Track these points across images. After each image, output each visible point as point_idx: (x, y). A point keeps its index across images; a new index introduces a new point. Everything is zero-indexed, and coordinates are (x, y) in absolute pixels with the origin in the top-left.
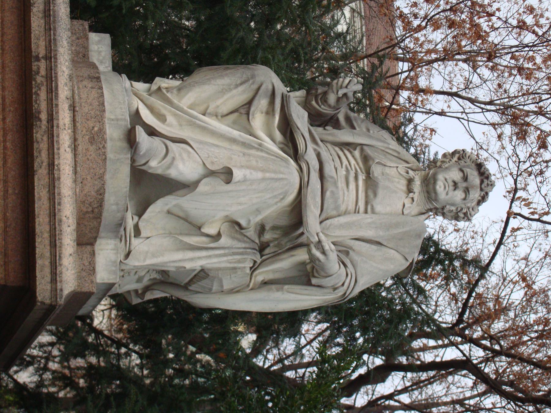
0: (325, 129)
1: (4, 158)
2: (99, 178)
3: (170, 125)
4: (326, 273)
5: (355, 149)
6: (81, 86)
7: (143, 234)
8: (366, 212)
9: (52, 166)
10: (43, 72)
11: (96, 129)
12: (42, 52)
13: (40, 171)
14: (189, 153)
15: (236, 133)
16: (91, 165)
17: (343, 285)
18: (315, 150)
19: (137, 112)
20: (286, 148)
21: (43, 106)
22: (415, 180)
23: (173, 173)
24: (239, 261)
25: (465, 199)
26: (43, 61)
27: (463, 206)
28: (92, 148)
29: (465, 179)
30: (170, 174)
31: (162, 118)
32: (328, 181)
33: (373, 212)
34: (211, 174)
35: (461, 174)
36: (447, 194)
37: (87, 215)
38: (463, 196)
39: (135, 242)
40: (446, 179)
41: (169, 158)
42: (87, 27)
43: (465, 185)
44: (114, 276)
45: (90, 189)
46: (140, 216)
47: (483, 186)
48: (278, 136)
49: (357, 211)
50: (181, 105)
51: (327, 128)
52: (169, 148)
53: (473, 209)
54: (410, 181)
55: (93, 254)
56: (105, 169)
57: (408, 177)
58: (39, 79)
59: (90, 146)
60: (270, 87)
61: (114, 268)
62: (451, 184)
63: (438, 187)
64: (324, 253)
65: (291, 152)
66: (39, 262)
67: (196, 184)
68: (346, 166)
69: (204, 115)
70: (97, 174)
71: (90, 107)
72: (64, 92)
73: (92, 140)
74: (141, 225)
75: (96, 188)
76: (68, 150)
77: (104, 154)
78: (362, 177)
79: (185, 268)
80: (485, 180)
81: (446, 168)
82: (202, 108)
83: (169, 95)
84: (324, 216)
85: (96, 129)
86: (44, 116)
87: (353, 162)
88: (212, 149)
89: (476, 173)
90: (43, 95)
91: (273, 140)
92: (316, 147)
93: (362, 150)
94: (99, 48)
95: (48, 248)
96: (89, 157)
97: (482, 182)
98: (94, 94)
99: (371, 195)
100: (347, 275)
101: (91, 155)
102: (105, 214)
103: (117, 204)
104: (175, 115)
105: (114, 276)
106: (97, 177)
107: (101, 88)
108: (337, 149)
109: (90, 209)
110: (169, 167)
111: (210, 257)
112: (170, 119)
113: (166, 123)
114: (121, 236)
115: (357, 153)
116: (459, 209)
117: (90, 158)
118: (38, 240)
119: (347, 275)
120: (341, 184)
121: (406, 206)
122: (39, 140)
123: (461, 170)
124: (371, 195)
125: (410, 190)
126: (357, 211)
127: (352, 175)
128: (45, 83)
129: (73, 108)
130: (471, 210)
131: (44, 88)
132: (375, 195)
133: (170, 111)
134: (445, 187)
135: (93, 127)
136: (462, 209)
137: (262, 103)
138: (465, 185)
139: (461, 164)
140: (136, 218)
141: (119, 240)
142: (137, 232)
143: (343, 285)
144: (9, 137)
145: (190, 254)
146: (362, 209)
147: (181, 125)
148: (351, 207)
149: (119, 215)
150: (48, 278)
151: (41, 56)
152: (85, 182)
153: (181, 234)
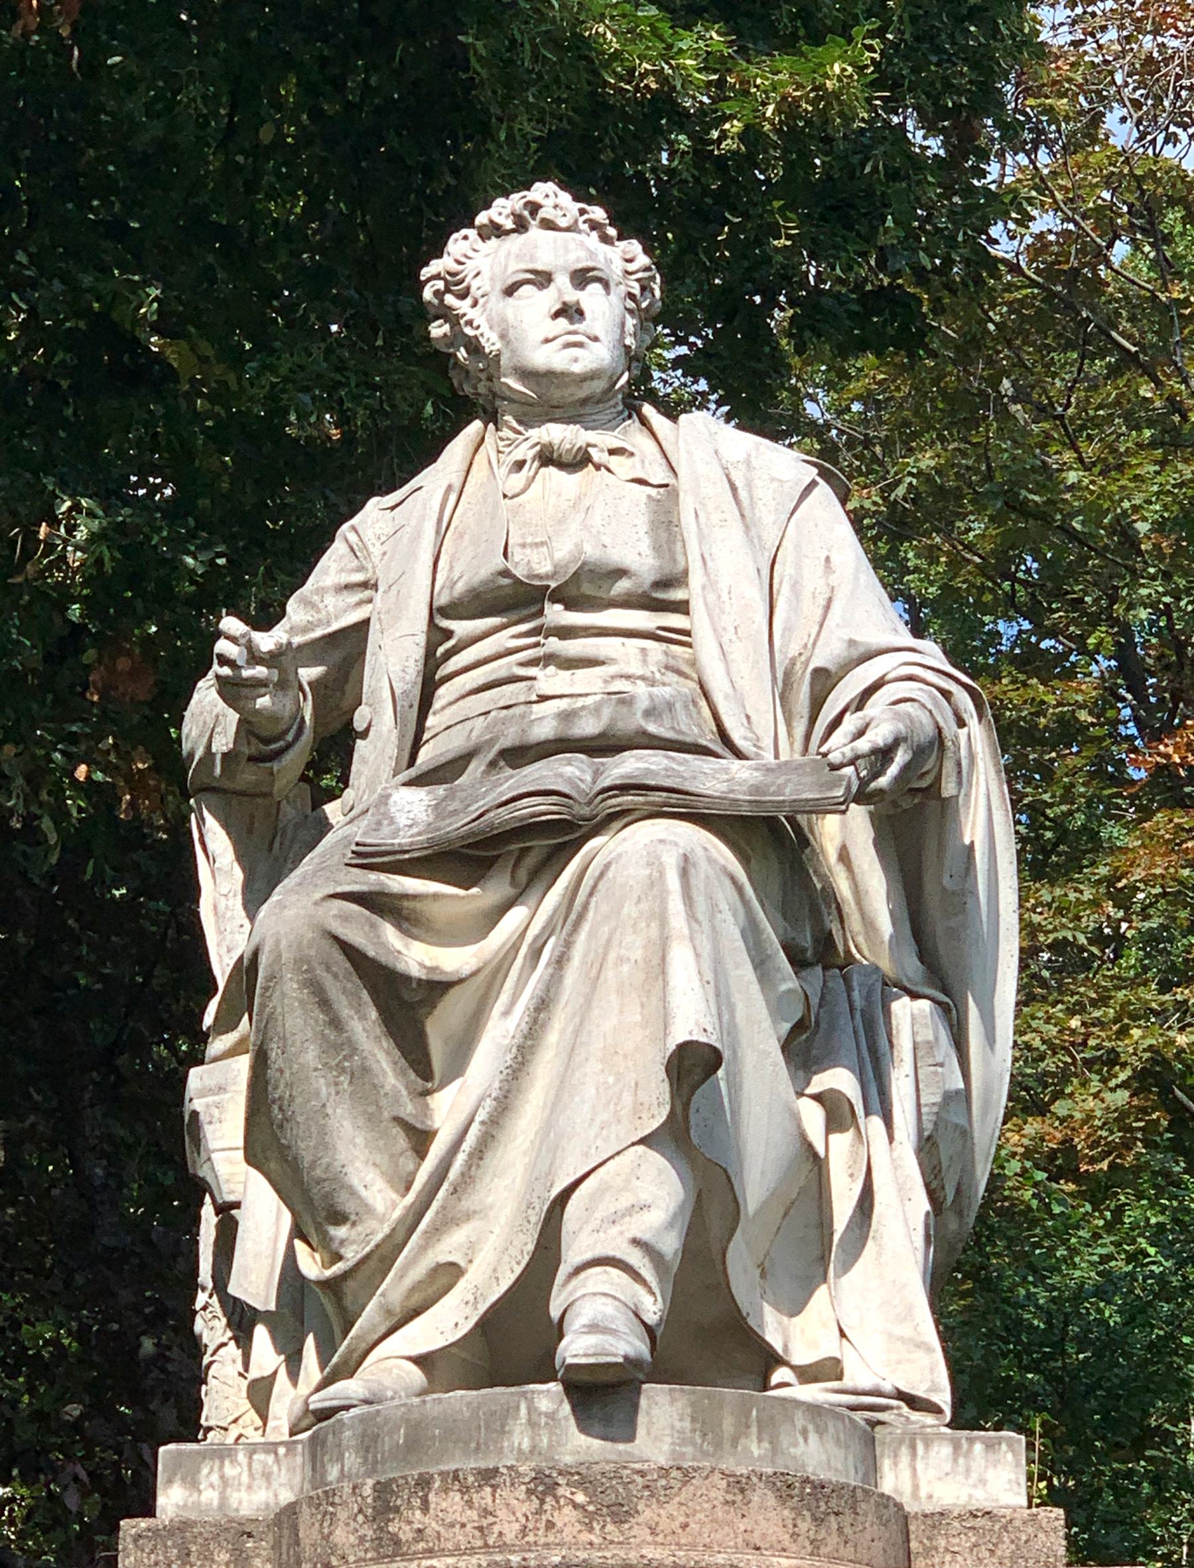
0: (364, 735)
2: (742, 1491)
3: (472, 1247)
4: (931, 743)
5: (449, 634)
8: (682, 607)
11: (580, 1498)
14: (604, 1189)
16: (700, 1516)
17: (946, 694)
19: (420, 1361)
20: (530, 861)
22: (545, 439)
23: (670, 1245)
25: (606, 285)
27: (623, 289)
28: (647, 1514)
29: (543, 279)
30: (676, 1253)
32: (610, 726)
35: (526, 290)
36: (596, 339)
37: (848, 1530)
38: (596, 287)
39: (857, 1375)
40: (547, 341)
41: (636, 1258)
42: (143, 1523)
43: (562, 281)
44: (1004, 1447)
47: (563, 223)
50: (397, 1214)
51: (359, 724)
52: (588, 1256)
53: (630, 261)
54: (548, 457)
57: (536, 464)
59: (640, 1519)
61: (978, 1447)
62: (562, 322)
63: (577, 368)
65: (542, 844)
68: (522, 664)
70: (730, 1497)
73: (620, 1513)
74: (802, 1356)
75: (771, 1501)
78: (556, 614)
79: (928, 1213)
80: (542, 214)
81: (503, 337)
82: (402, 1141)
83: (352, 1255)
84: (718, 748)
85: (580, 1498)
87: (504, 639)
89: (515, 242)
92: (476, 767)
93: (454, 610)
94: (212, 1486)
96: (677, 1523)
97: (548, 225)
99: (622, 586)
100: (911, 678)
101: (671, 1517)
104: (436, 1231)
105: (1004, 1447)
106: (739, 1497)
108: (444, 694)
112: (448, 1249)
113: (462, 1264)
114: (868, 1422)
115: (462, 628)
116: (631, 304)
117: (682, 1519)
119: (911, 678)
120: (586, 680)
121: (641, 475)
123: (510, 291)
124: (622, 586)
127: (553, 644)
130: (631, 267)
133: (423, 1249)
134: (579, 345)
135: (576, 1506)
136: (631, 296)
139: (486, 288)
140: (781, 1375)
141: (878, 1428)
142: (827, 1370)
143: (946, 694)
146: (675, 620)
147: (468, 1216)
152: (756, 1539)
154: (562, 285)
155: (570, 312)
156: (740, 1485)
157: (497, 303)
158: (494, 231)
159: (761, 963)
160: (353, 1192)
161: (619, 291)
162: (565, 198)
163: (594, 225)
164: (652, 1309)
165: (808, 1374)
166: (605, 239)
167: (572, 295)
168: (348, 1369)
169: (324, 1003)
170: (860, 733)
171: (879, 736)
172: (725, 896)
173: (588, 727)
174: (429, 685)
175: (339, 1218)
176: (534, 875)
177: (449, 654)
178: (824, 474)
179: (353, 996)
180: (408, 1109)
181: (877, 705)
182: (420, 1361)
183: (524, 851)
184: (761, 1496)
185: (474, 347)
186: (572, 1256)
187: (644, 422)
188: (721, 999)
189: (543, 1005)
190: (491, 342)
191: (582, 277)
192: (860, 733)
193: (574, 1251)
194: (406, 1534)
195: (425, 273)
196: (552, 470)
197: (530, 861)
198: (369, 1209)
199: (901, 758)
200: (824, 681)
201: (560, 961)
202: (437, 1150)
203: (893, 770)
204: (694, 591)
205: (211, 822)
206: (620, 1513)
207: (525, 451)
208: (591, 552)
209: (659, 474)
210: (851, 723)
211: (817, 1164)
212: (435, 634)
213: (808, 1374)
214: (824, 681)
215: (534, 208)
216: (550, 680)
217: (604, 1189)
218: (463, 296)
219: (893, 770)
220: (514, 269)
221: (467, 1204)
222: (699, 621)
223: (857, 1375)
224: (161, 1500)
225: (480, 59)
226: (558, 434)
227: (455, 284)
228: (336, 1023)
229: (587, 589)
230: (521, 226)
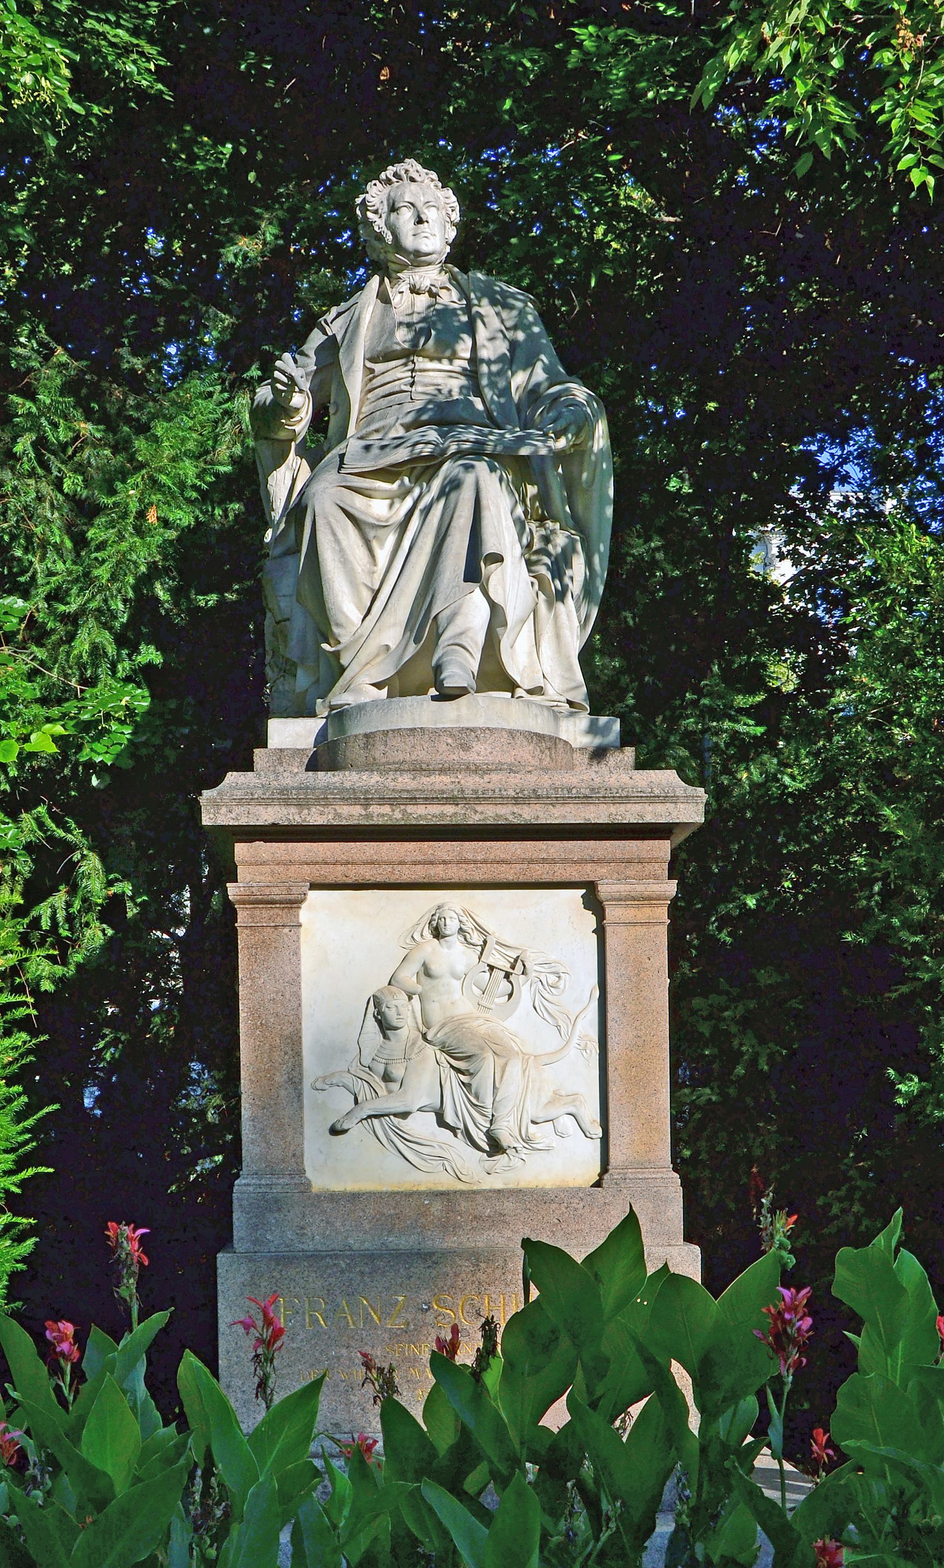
1: (498, 862)
6: (384, 760)
10: (386, 809)
11: (450, 741)
13: (525, 816)
20: (416, 473)
21: (435, 809)
26: (371, 809)
28: (477, 747)
39: (551, 691)
56: (503, 729)
66: (649, 819)
67: (493, 606)
71: (418, 748)
72: (405, 781)
73: (466, 747)
75: (525, 743)
85: (450, 741)
86: (449, 809)
88: (445, 581)
95: (629, 806)
98: (395, 742)
102: (545, 732)
103: (536, 715)
107: (385, 733)
109: (547, 752)
110: (476, 643)
118: (619, 820)
122: (482, 817)
128: (403, 807)
131: (410, 809)
149: (546, 712)
150: (670, 806)
151: (364, 813)
160: (343, 613)
165: (530, 692)
183: (414, 468)
184: (520, 740)
185: (379, 237)
190: (389, 238)
194: (378, 755)
197: (416, 473)
206: (466, 747)
224: (269, 741)
225: (513, 296)
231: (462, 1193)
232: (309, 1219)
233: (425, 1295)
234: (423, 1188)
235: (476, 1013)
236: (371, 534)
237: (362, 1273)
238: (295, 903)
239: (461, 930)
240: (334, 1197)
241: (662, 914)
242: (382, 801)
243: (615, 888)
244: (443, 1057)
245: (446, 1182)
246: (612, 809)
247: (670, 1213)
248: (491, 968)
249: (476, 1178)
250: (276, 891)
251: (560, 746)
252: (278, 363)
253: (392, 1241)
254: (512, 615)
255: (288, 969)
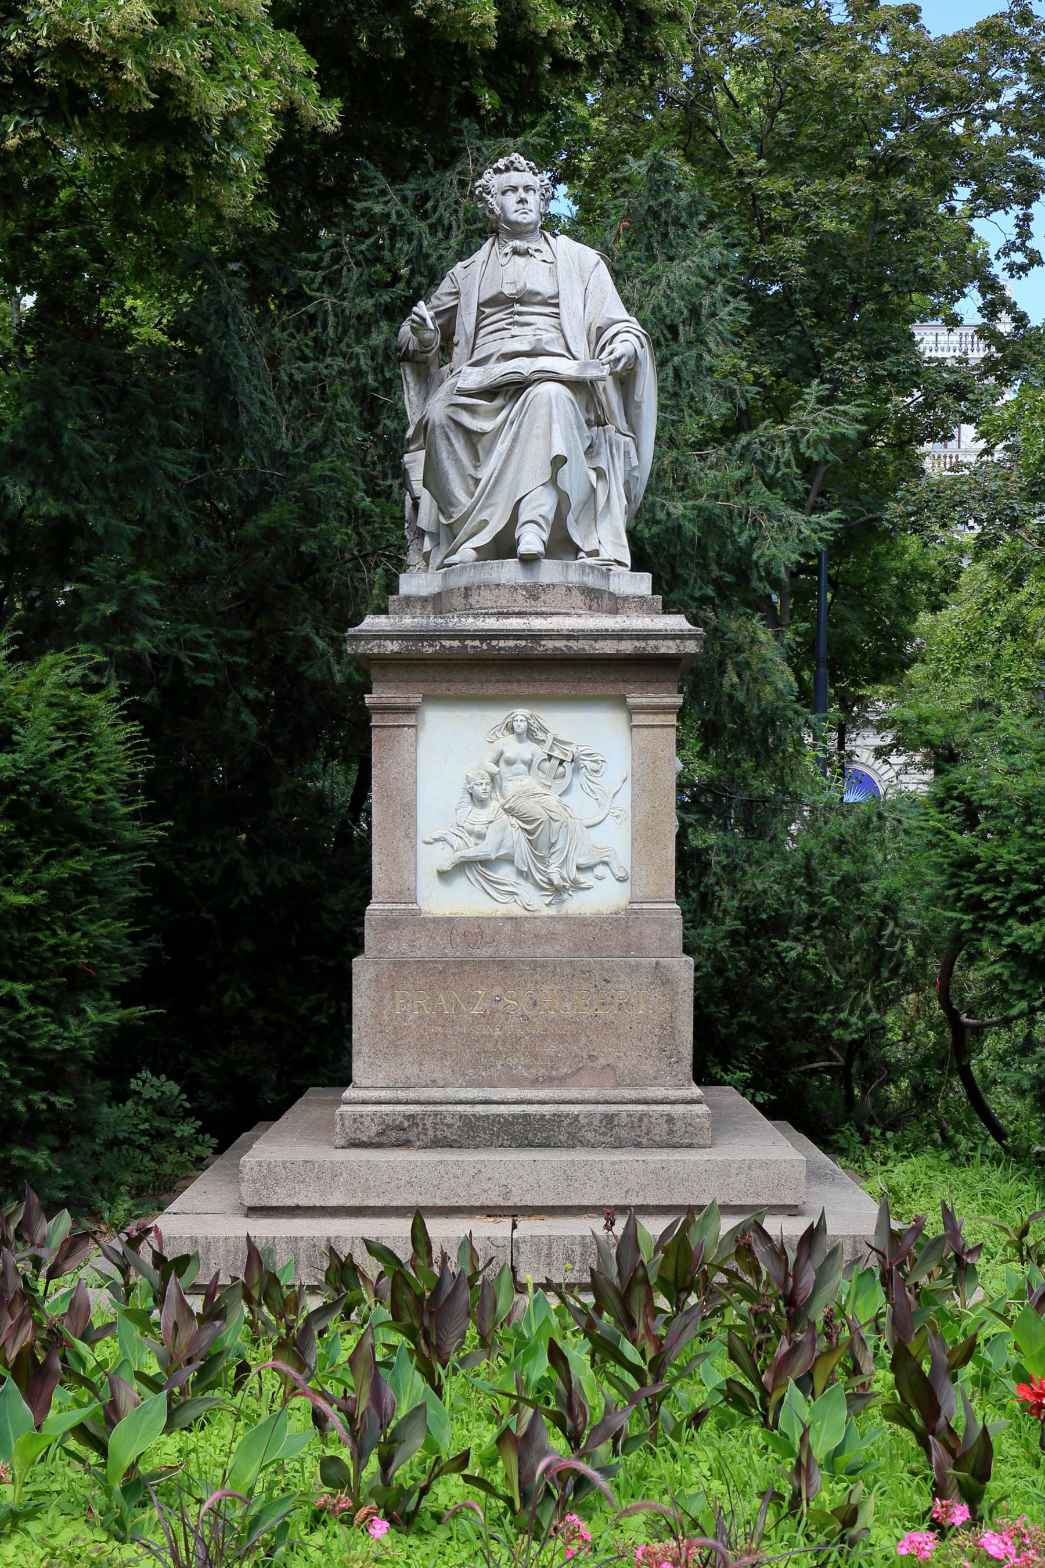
3: (492, 515)
7: (597, 547)
8: (557, 305)
9: (569, 637)
10: (477, 643)
12: (456, 643)
15: (501, 447)
18: (498, 360)
19: (475, 549)
21: (511, 643)
23: (551, 517)
24: (618, 449)
28: (543, 597)
29: (515, 189)
31: (484, 523)
33: (557, 296)
34: (553, 481)
39: (604, 555)
43: (521, 190)
45: (578, 599)
46: (578, 550)
48: (498, 402)
49: (556, 316)
54: (516, 252)
55: (626, 599)
58: (485, 647)
60: (453, 408)
62: (521, 206)
64: (618, 360)
65: (513, 388)
69: (477, 481)
72: (492, 623)
73: (536, 598)
76: (549, 620)
77: (548, 586)
78: (518, 308)
82: (471, 482)
83: (456, 516)
89: (505, 175)
90: (502, 644)
91: (502, 408)
97: (517, 169)
104: (481, 510)
108: (482, 332)
111: (616, 478)
112: (484, 516)
115: (488, 311)
123: (504, 193)
125: (526, 253)
126: (556, 316)
127: (517, 318)
129: (508, 614)
131: (494, 643)
132: (538, 294)
137: (466, 419)
138: (521, 190)
140: (582, 554)
142: (595, 553)
144: (536, 676)
145: (615, 500)
146: (555, 310)
148: (553, 321)
153: (595, 509)
154: (521, 193)
155: (522, 201)
156: (569, 589)
157: (499, 197)
158: (498, 171)
159: (579, 428)
161: (538, 193)
162: (522, 159)
163: (531, 169)
164: (545, 537)
165: (590, 554)
166: (535, 174)
167: (524, 195)
168: (454, 552)
169: (448, 439)
170: (611, 353)
171: (616, 354)
172: (569, 407)
173: (526, 347)
174: (477, 329)
175: (452, 505)
176: (511, 398)
177: (484, 319)
178: (602, 257)
179: (457, 438)
180: (472, 471)
181: (616, 344)
182: (475, 549)
184: (575, 592)
185: (492, 211)
186: (522, 519)
187: (546, 239)
188: (567, 440)
189: (515, 440)
190: (498, 210)
191: (527, 188)
192: (611, 353)
193: (522, 518)
194: (473, 602)
195: (477, 184)
196: (516, 257)
198: (459, 502)
199: (623, 361)
200: (601, 331)
201: (520, 426)
202: (482, 484)
203: (621, 365)
204: (562, 300)
205: (408, 371)
207: (508, 250)
208: (529, 286)
209: (550, 259)
210: (608, 349)
211: (594, 490)
212: (480, 312)
213: (590, 554)
214: (601, 331)
215: (512, 163)
216: (515, 330)
217: (531, 499)
218: (488, 193)
219: (621, 365)
220: (505, 185)
221: (490, 502)
222: (563, 310)
223: (604, 555)
226: (517, 243)
227: (487, 190)
228: (451, 445)
229: (526, 299)
230: (507, 169)
231: (526, 918)
232: (417, 935)
233: (498, 990)
234: (499, 914)
235: (539, 789)
236: (475, 440)
237: (454, 974)
238: (410, 710)
239: (529, 729)
240: (436, 921)
241: (672, 720)
242: (473, 637)
243: (638, 700)
244: (514, 820)
245: (517, 911)
246: (637, 644)
247: (673, 935)
248: (550, 757)
249: (536, 907)
250: (399, 700)
251: (606, 596)
252: (415, 309)
253: (476, 952)
254: (575, 499)
255: (407, 756)
